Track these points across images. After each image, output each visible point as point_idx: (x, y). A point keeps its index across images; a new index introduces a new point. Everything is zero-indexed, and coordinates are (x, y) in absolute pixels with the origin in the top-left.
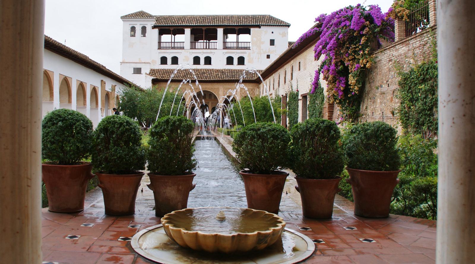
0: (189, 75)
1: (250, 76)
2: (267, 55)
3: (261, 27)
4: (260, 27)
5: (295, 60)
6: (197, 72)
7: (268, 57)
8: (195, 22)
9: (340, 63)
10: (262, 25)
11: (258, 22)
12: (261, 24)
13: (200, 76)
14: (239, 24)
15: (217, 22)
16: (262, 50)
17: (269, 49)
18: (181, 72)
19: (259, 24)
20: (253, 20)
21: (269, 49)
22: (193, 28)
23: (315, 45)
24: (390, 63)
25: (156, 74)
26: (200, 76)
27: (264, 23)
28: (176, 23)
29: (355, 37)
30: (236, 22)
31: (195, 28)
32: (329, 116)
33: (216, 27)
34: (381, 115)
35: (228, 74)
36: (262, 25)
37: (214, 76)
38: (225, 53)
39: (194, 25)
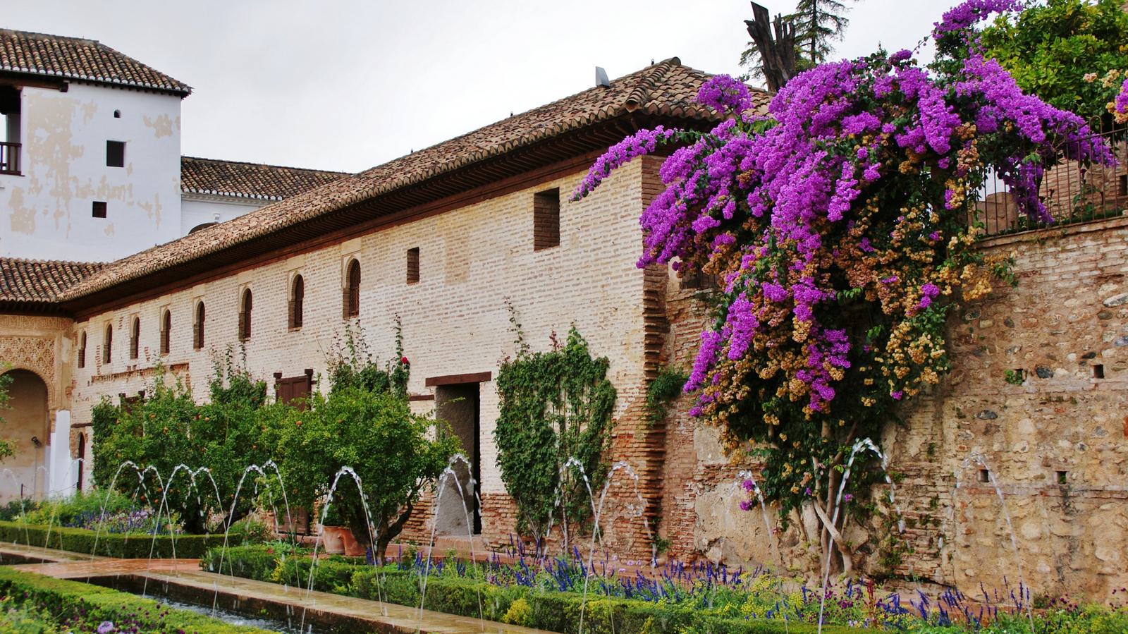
2: (95, 204)
3: (72, 87)
5: (377, 238)
7: (99, 210)
9: (828, 275)
10: (73, 80)
11: (56, 65)
16: (75, 179)
17: (104, 178)
20: (28, 55)
21: (104, 178)
23: (536, 189)
24: (1111, 287)
27: (82, 71)
29: (902, 176)
32: (650, 472)
34: (1051, 479)
36: (73, 80)
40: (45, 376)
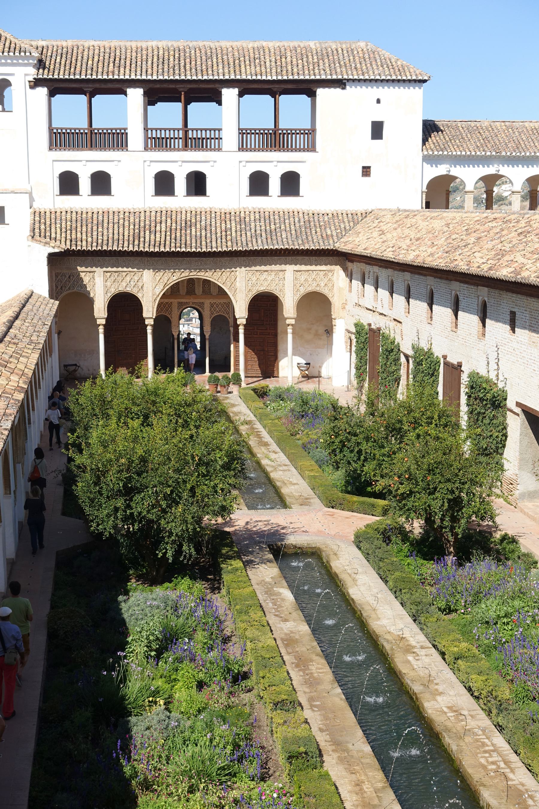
0: (147, 232)
1: (319, 234)
4: (345, 84)
6: (169, 220)
7: (366, 171)
8: (155, 68)
10: (348, 80)
12: (346, 77)
13: (178, 234)
14: (285, 78)
15: (221, 66)
18: (121, 221)
19: (340, 77)
22: (151, 86)
25: (53, 230)
26: (178, 234)
27: (355, 73)
28: (100, 70)
30: (274, 71)
31: (158, 86)
33: (217, 86)
35: (258, 228)
37: (219, 235)
38: (244, 163)
39: (155, 77)
40: (329, 296)
